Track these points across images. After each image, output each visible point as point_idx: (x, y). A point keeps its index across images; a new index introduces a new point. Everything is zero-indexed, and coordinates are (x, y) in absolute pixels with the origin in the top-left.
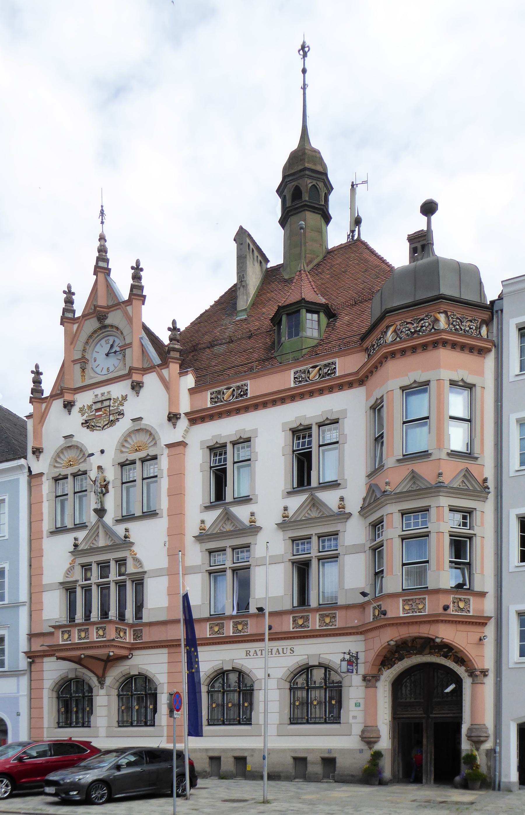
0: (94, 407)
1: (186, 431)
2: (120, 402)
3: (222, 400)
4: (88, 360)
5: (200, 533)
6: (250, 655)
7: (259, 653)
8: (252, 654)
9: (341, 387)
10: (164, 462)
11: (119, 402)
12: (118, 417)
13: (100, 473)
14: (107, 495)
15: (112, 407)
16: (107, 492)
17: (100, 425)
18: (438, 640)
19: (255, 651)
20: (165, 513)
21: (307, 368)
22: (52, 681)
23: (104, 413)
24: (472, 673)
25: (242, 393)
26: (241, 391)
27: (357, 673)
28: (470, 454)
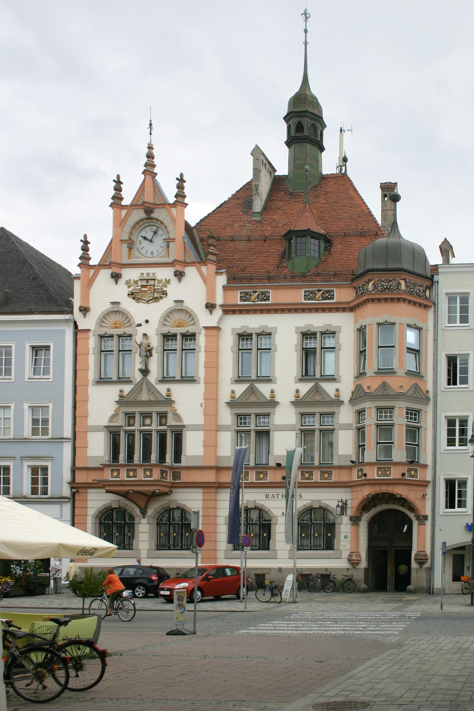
0: (140, 283)
1: (221, 319)
2: (164, 284)
3: (250, 300)
4: (134, 242)
5: (231, 400)
6: (269, 498)
7: (276, 496)
8: (270, 496)
9: (337, 310)
10: (201, 340)
11: (162, 284)
12: (162, 296)
13: (145, 340)
14: (151, 358)
15: (157, 286)
16: (151, 355)
17: (146, 299)
18: (398, 496)
19: (273, 495)
20: (202, 381)
21: (314, 290)
22: (96, 509)
23: (150, 290)
24: (418, 518)
25: (265, 298)
26: (265, 296)
27: (346, 514)
28: (419, 373)
